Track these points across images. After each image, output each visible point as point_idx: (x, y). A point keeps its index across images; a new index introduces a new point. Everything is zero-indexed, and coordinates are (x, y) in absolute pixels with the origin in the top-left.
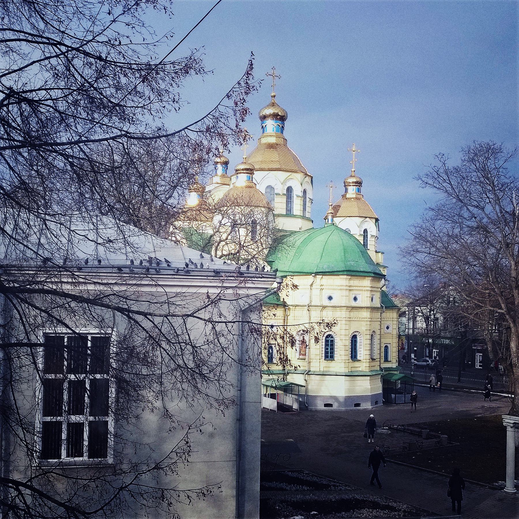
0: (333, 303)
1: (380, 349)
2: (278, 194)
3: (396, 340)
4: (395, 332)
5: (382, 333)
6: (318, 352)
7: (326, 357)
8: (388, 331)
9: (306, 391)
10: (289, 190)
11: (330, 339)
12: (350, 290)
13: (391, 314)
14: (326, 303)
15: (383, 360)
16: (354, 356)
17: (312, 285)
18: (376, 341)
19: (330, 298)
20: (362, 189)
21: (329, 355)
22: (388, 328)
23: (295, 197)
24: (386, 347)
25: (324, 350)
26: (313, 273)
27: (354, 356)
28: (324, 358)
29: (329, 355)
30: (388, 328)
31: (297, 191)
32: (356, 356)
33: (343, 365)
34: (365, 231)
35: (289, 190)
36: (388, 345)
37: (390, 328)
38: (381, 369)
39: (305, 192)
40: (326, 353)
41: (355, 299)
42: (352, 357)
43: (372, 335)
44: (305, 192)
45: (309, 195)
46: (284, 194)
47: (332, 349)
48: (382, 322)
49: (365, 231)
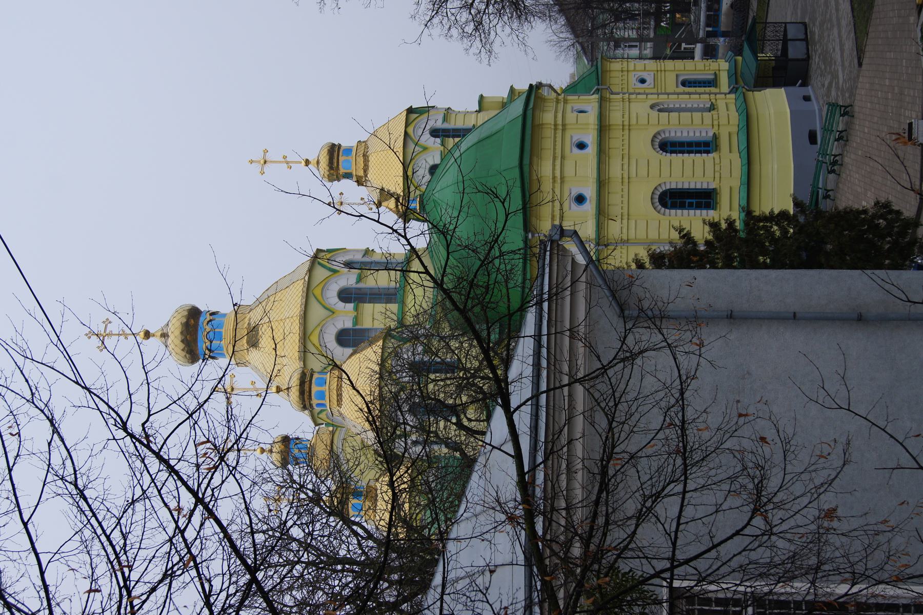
0: (590, 192)
1: (689, 94)
2: (356, 320)
3: (669, 64)
4: (652, 65)
5: (655, 91)
8: (650, 80)
10: (345, 295)
12: (563, 157)
13: (613, 74)
14: (589, 207)
15: (713, 90)
16: (705, 146)
18: (672, 101)
20: (345, 144)
22: (643, 81)
23: (361, 285)
24: (684, 83)
26: (526, 237)
27: (705, 146)
30: (643, 81)
31: (348, 279)
32: (707, 144)
34: (435, 133)
35: (345, 295)
36: (681, 79)
37: (645, 75)
38: (733, 90)
39: (349, 265)
42: (708, 152)
43: (660, 111)
44: (349, 265)
45: (358, 257)
46: (356, 309)
48: (631, 91)
49: (435, 133)
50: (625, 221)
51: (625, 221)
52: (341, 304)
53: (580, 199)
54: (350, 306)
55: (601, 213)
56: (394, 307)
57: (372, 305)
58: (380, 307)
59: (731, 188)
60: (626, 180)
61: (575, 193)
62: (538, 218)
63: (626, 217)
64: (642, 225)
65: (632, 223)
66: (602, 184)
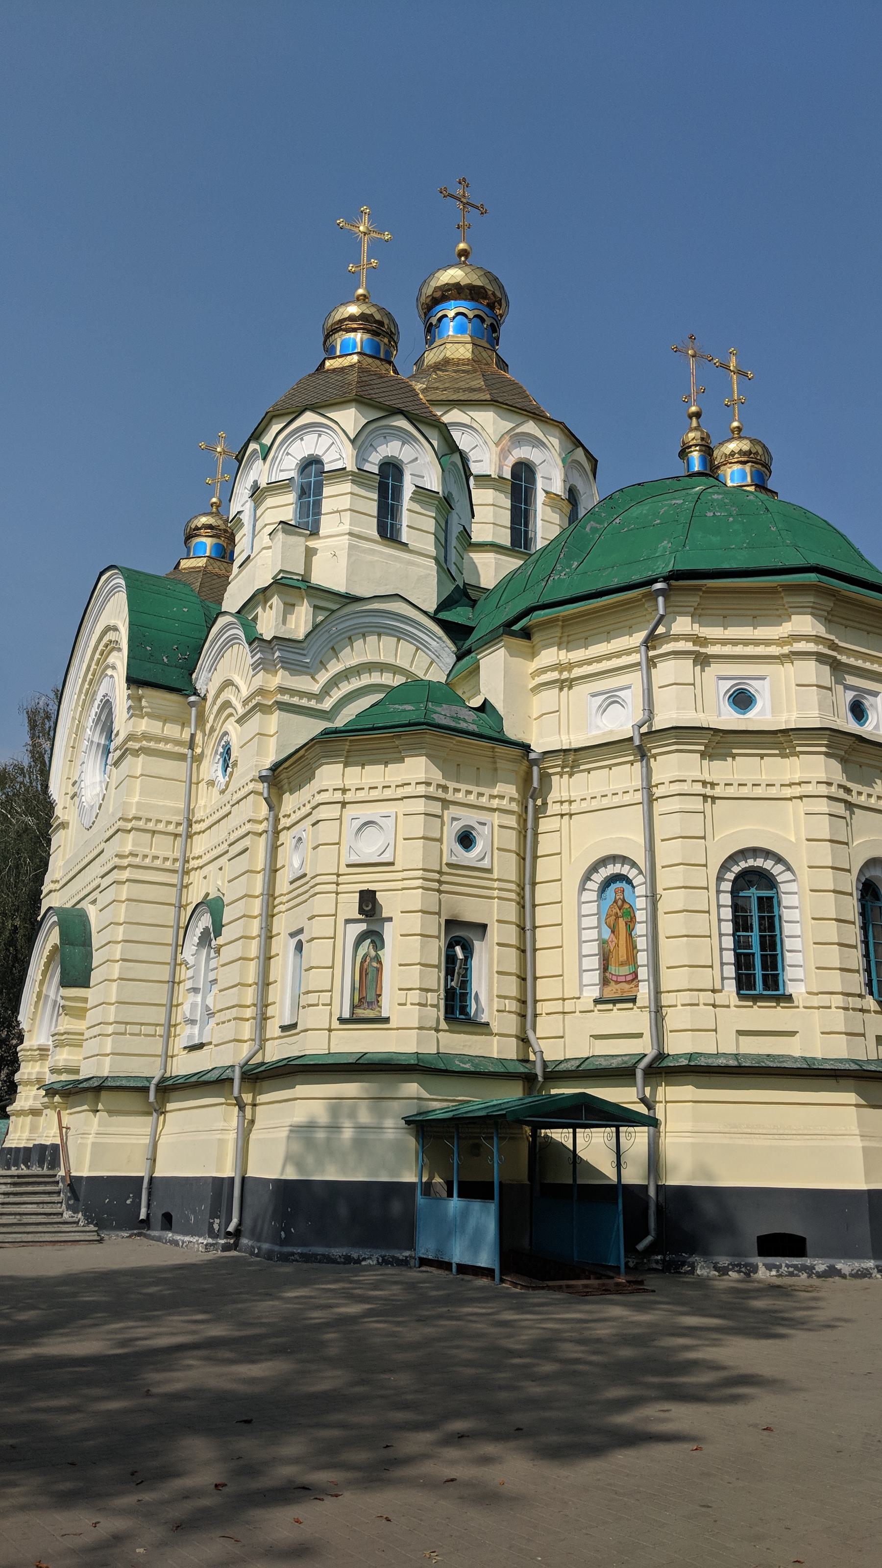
2: (484, 479)
6: (705, 951)
7: (744, 983)
9: (654, 1160)
11: (754, 893)
14: (729, 718)
17: (651, 641)
19: (742, 700)
21: (759, 972)
23: (540, 497)
25: (729, 942)
26: (655, 581)
28: (731, 986)
29: (759, 972)
33: (838, 1020)
40: (742, 962)
41: (858, 711)
47: (771, 944)
50: (698, 788)
51: (698, 788)
52: (511, 461)
53: (742, 700)
54: (508, 475)
55: (718, 743)
56: (505, 539)
57: (509, 506)
58: (506, 518)
59: (793, 1034)
60: (797, 791)
61: (753, 687)
62: (698, 616)
63: (708, 791)
64: (695, 826)
65: (697, 804)
66: (782, 741)
